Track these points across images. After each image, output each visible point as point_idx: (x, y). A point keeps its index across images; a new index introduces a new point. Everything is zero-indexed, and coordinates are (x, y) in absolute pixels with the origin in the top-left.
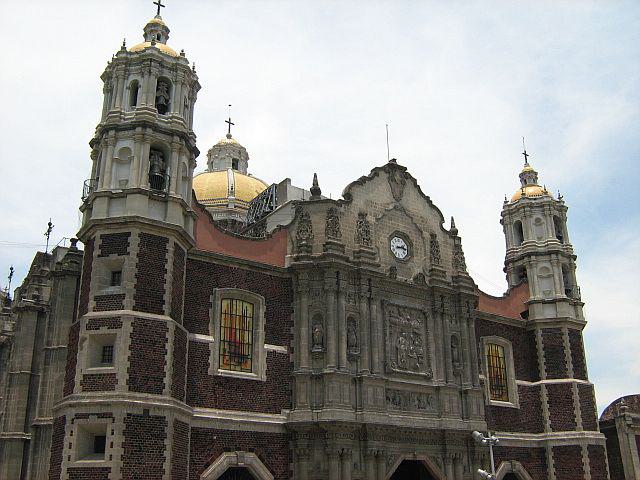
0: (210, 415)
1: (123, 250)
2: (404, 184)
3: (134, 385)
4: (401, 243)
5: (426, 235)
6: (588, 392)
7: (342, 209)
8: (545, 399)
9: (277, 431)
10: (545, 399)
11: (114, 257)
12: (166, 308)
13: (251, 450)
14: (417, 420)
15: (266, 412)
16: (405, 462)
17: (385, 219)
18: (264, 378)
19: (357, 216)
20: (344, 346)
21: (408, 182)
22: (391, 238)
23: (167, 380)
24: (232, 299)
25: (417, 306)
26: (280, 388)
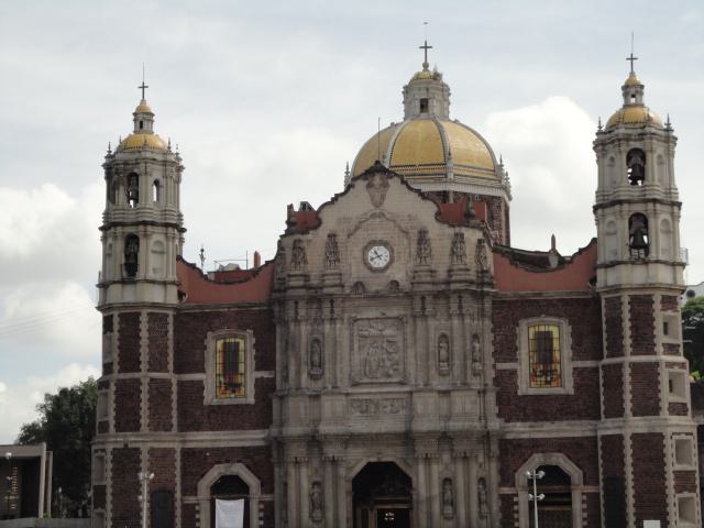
0: (203, 439)
1: (112, 331)
2: (386, 185)
3: (119, 428)
4: (371, 254)
7: (309, 236)
8: (601, 381)
9: (262, 443)
10: (601, 381)
11: (108, 333)
12: (141, 366)
13: (239, 461)
14: (389, 424)
16: (369, 464)
17: (359, 232)
18: (251, 400)
19: (326, 238)
21: (394, 183)
22: (366, 249)
25: (395, 312)
26: (263, 412)
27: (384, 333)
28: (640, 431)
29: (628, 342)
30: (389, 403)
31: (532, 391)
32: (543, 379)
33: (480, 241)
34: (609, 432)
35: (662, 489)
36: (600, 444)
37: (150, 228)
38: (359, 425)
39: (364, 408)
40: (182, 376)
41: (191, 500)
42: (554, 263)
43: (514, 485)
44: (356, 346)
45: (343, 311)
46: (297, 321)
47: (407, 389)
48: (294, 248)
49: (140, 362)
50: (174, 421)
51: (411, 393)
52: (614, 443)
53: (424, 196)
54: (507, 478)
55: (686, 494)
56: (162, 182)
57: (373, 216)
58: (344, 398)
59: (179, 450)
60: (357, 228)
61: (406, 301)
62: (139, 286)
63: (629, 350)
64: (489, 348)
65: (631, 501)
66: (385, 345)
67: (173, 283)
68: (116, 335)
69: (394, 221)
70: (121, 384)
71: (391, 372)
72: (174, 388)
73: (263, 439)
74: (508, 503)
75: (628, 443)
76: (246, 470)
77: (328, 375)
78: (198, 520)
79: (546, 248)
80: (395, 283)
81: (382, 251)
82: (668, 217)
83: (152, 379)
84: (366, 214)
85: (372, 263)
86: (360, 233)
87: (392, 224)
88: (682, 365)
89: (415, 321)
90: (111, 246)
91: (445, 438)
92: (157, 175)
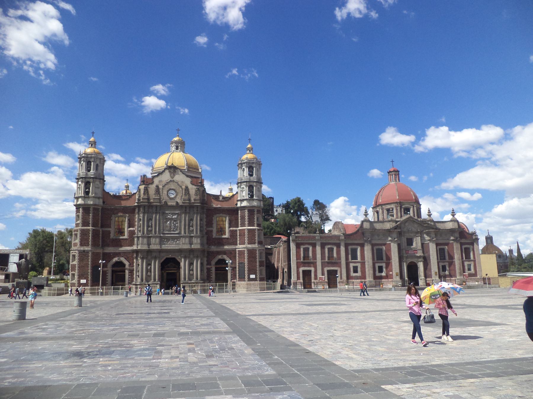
2: (175, 172)
3: (81, 245)
4: (170, 192)
5: (184, 187)
8: (238, 234)
10: (238, 234)
11: (78, 214)
12: (90, 225)
13: (122, 257)
15: (128, 246)
16: (167, 258)
23: (90, 243)
24: (118, 217)
27: (173, 217)
28: (250, 249)
29: (246, 223)
31: (217, 237)
32: (220, 233)
33: (203, 190)
34: (241, 249)
35: (256, 266)
36: (237, 252)
37: (95, 179)
38: (164, 247)
40: (103, 229)
41: (105, 269)
42: (221, 198)
43: (211, 265)
45: (160, 210)
48: (144, 189)
49: (90, 224)
50: (101, 243)
51: (181, 236)
52: (241, 253)
53: (187, 176)
54: (209, 263)
55: (262, 267)
56: (99, 164)
57: (171, 181)
59: (102, 253)
60: (165, 184)
62: (90, 198)
63: (247, 225)
64: (205, 223)
65: (246, 269)
67: (101, 198)
68: (80, 214)
69: (178, 183)
70: (82, 231)
71: (175, 230)
72: (101, 233)
74: (209, 270)
76: (125, 260)
78: (108, 276)
79: (219, 194)
80: (177, 202)
81: (173, 192)
82: (259, 187)
83: (94, 229)
84: (168, 180)
85: (169, 194)
86: (167, 186)
87: (177, 184)
88: (262, 230)
90: (80, 185)
91: (191, 251)
92: (98, 162)
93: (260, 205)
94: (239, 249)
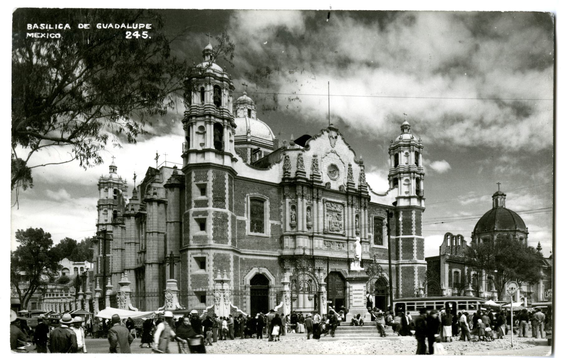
6: (421, 242)
19: (312, 156)
20: (305, 220)
25: (340, 201)
30: (337, 244)
36: (400, 270)
39: (329, 245)
44: (326, 215)
46: (303, 196)
47: (346, 238)
51: (348, 240)
58: (323, 239)
61: (344, 197)
66: (337, 215)
73: (279, 257)
75: (416, 270)
77: (315, 227)
87: (338, 158)
89: (348, 207)
93: (421, 205)
94: (403, 265)
